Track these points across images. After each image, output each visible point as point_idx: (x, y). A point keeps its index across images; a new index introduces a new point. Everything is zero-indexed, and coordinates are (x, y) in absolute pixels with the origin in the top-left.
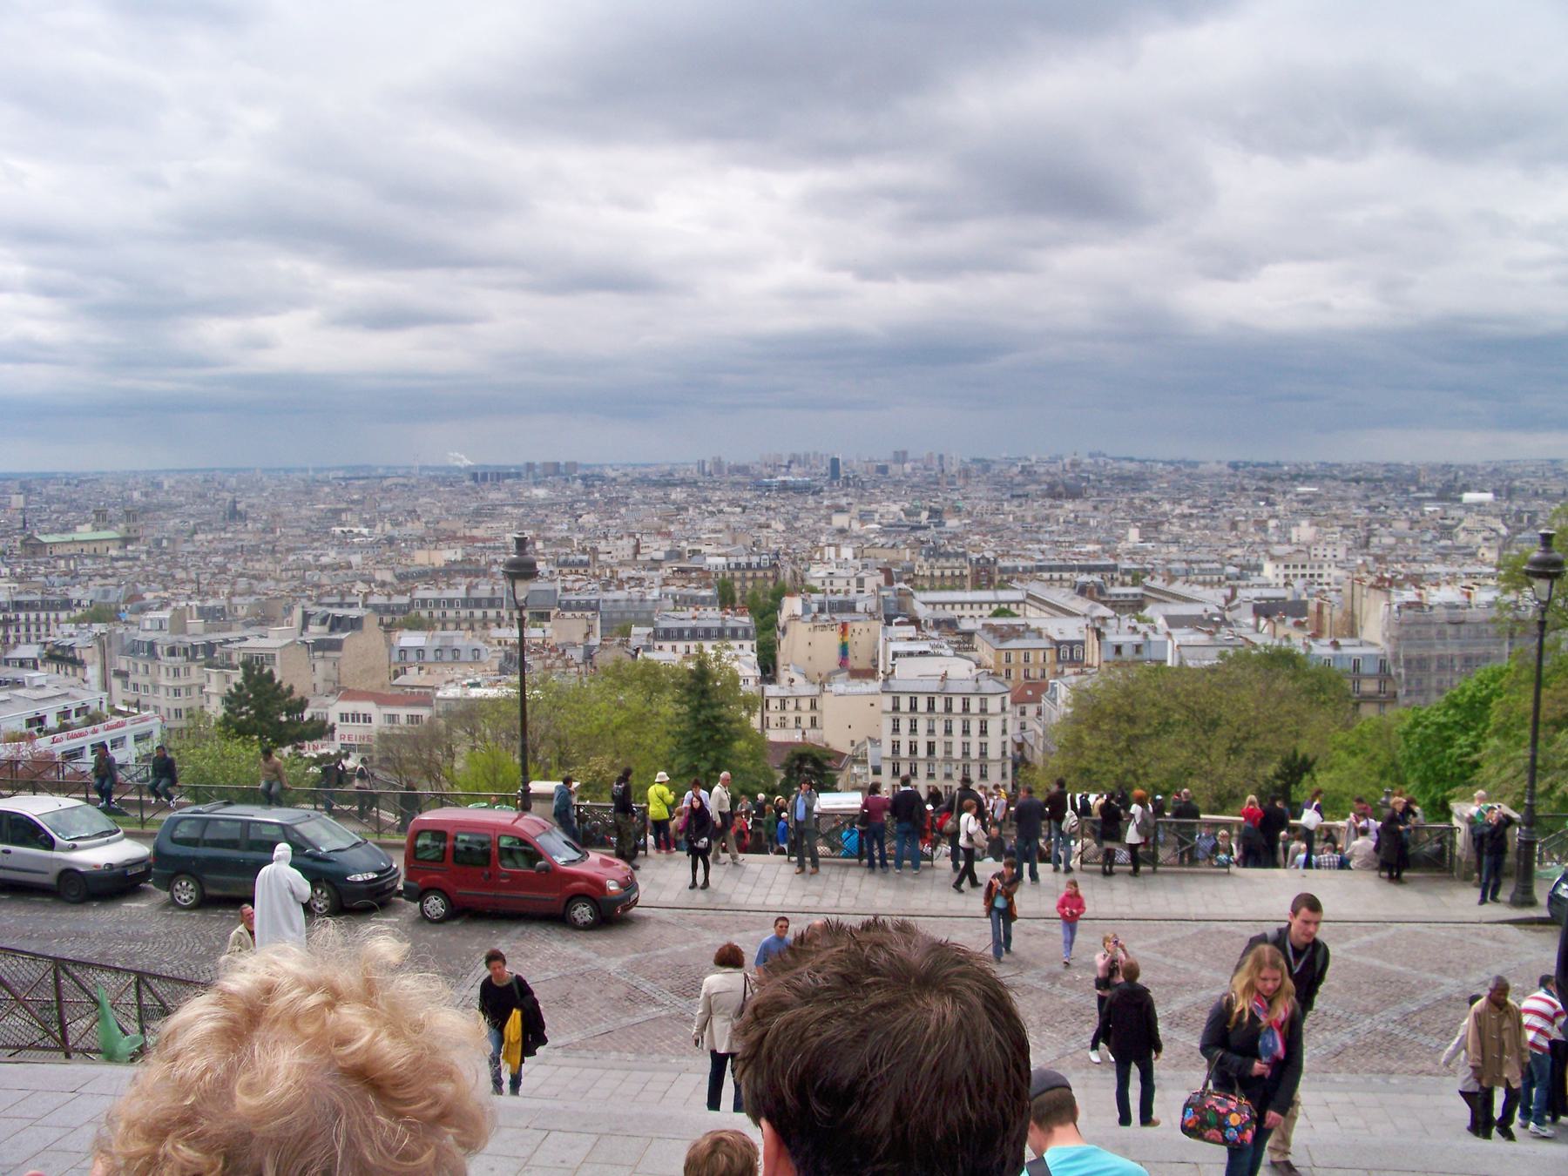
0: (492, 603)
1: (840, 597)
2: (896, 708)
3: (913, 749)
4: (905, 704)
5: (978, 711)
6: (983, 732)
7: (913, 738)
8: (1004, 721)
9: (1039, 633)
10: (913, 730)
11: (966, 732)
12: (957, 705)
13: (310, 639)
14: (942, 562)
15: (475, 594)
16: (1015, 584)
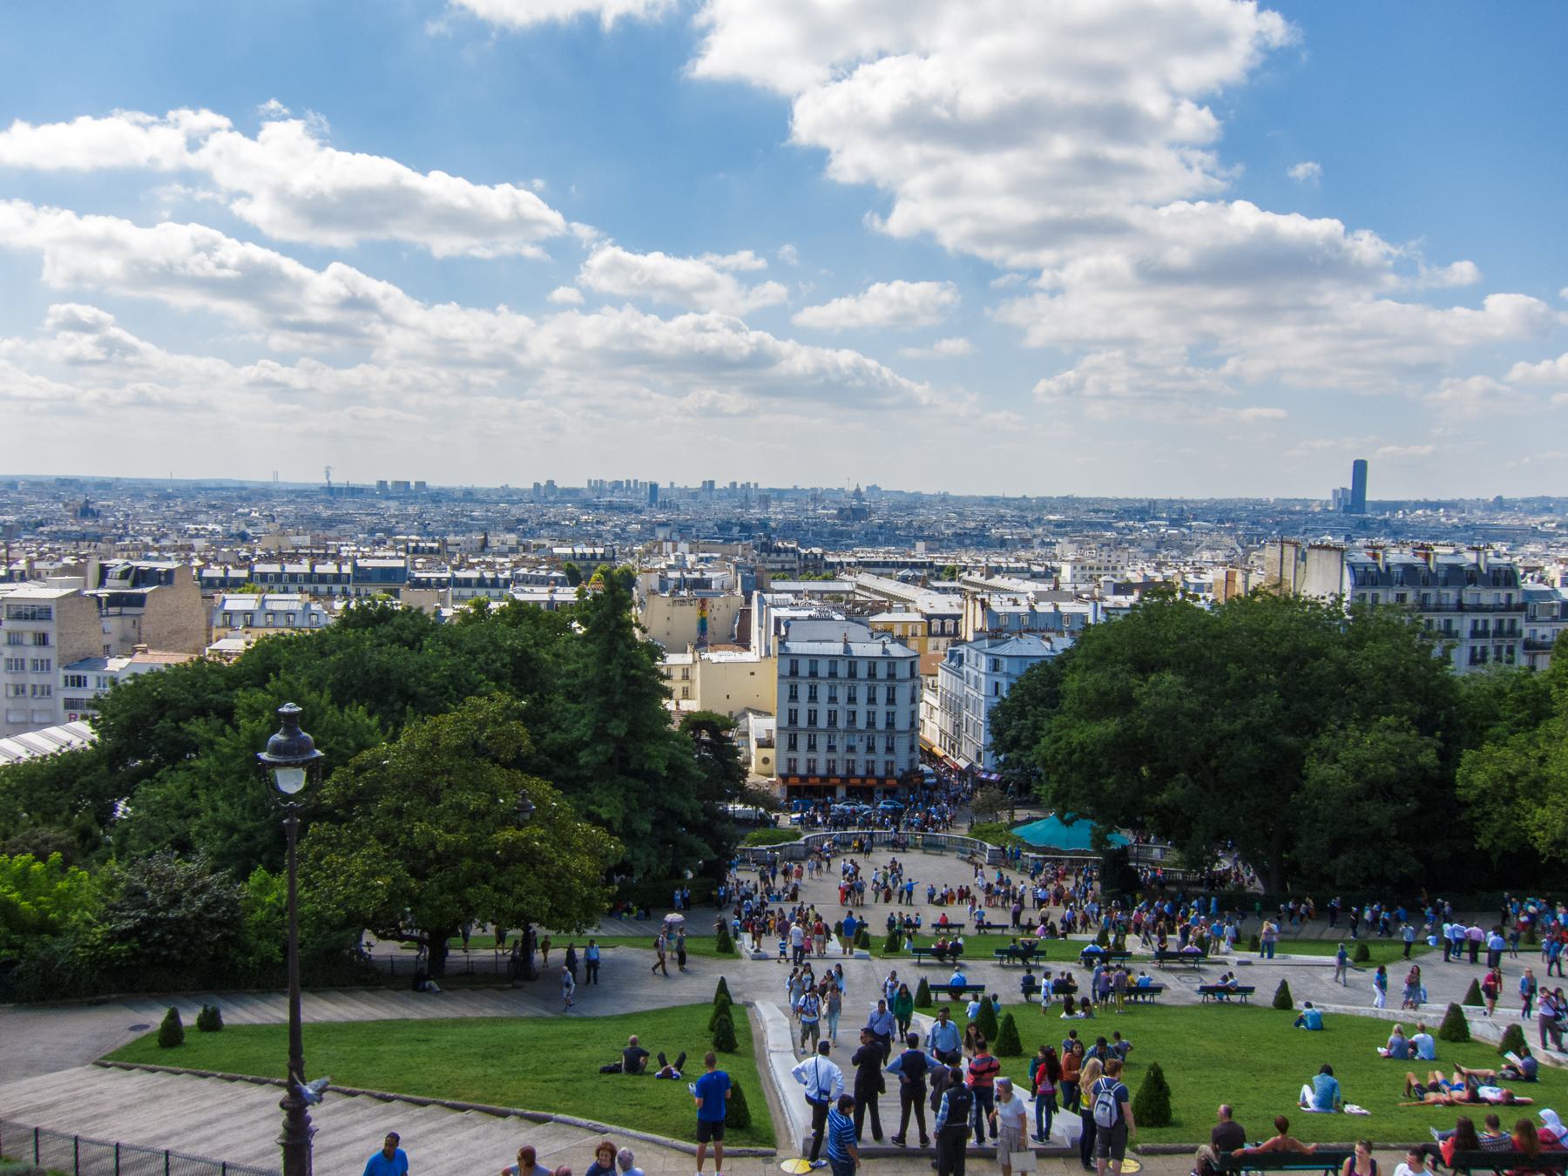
0: (337, 578)
1: (697, 575)
2: (794, 673)
3: (813, 719)
4: (804, 669)
5: (885, 677)
6: (891, 700)
7: (813, 706)
8: (914, 688)
9: (906, 604)
10: (813, 698)
11: (872, 700)
12: (862, 671)
13: (103, 593)
14: (773, 556)
15: (319, 569)
16: (844, 576)
